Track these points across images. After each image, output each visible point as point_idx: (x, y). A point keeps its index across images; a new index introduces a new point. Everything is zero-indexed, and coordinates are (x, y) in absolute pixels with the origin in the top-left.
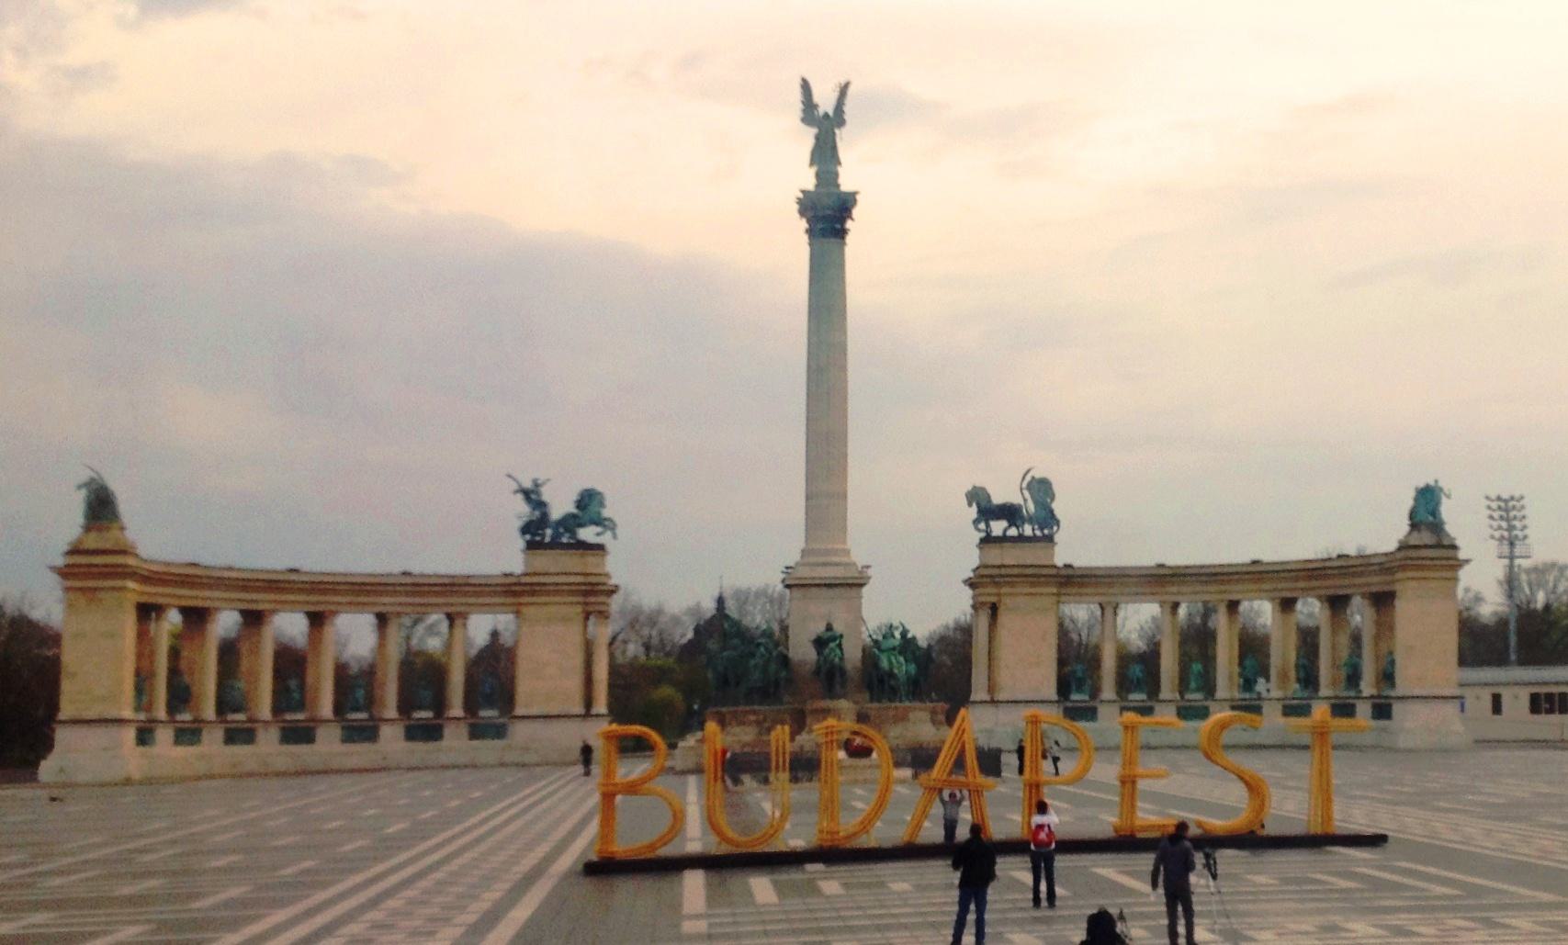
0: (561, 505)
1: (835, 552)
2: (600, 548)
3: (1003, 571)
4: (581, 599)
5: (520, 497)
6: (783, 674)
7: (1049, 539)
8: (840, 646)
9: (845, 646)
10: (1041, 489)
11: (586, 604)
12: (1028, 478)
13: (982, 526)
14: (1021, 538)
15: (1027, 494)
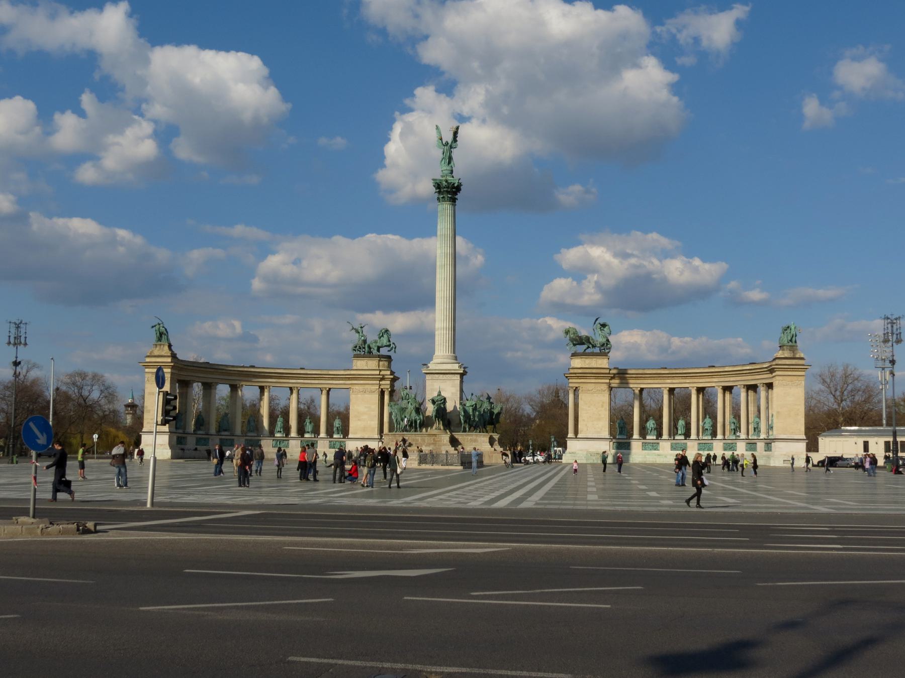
3: (580, 371)
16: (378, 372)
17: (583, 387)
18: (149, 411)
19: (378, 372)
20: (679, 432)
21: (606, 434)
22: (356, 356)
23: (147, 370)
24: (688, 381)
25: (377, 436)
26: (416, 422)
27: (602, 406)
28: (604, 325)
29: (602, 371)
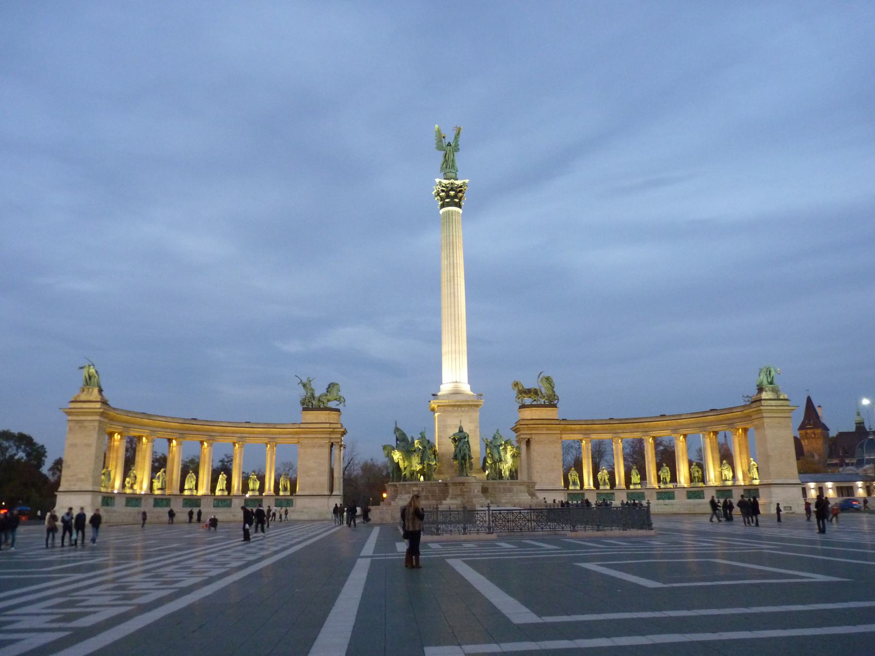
2: (338, 410)
3: (532, 422)
16: (328, 426)
17: (535, 438)
18: (69, 467)
19: (328, 426)
22: (304, 409)
23: (70, 418)
25: (327, 493)
27: (555, 457)
28: (548, 379)
29: (552, 422)
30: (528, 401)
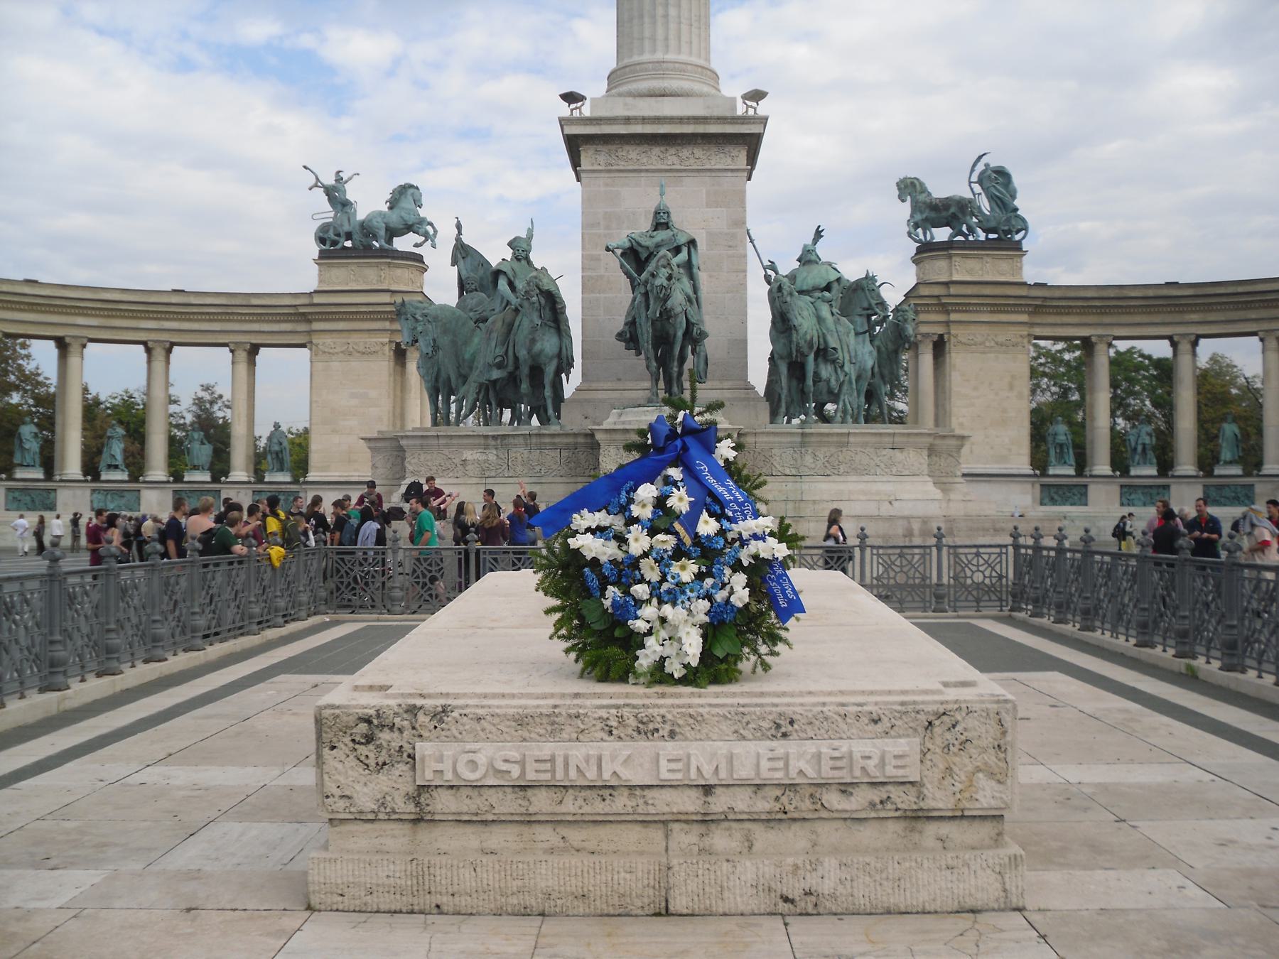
0: (369, 201)
1: (681, 69)
2: (419, 258)
3: (953, 290)
4: (387, 325)
5: (320, 192)
6: (548, 344)
7: (1017, 246)
8: (688, 266)
9: (702, 277)
10: (997, 182)
11: (393, 331)
12: (980, 167)
13: (920, 230)
14: (977, 246)
15: (977, 188)
16: (386, 298)
19: (386, 298)
20: (1226, 454)
21: (1022, 463)
24: (1253, 315)
26: (536, 372)
30: (942, 234)
